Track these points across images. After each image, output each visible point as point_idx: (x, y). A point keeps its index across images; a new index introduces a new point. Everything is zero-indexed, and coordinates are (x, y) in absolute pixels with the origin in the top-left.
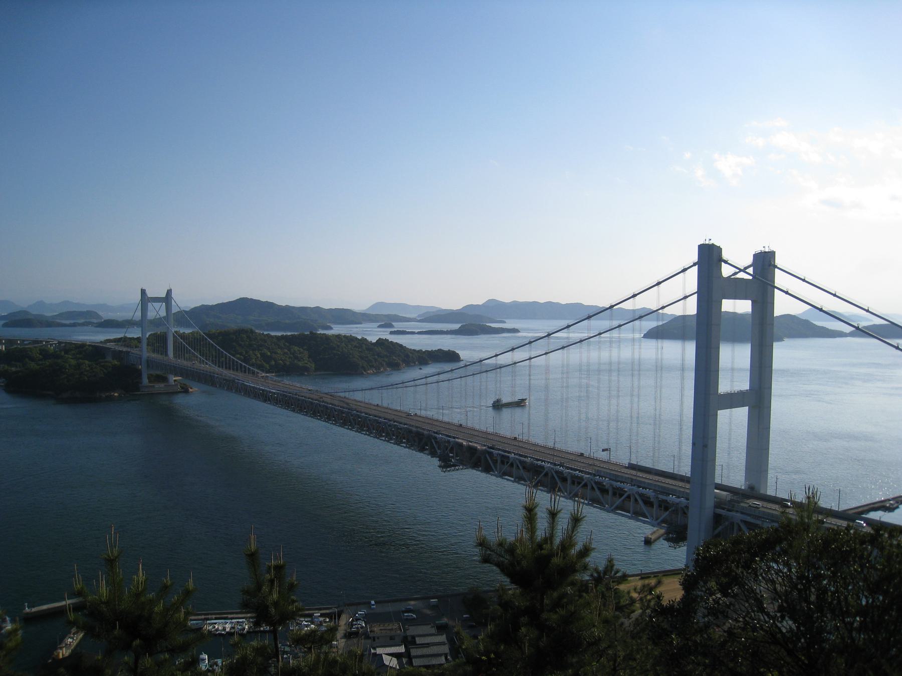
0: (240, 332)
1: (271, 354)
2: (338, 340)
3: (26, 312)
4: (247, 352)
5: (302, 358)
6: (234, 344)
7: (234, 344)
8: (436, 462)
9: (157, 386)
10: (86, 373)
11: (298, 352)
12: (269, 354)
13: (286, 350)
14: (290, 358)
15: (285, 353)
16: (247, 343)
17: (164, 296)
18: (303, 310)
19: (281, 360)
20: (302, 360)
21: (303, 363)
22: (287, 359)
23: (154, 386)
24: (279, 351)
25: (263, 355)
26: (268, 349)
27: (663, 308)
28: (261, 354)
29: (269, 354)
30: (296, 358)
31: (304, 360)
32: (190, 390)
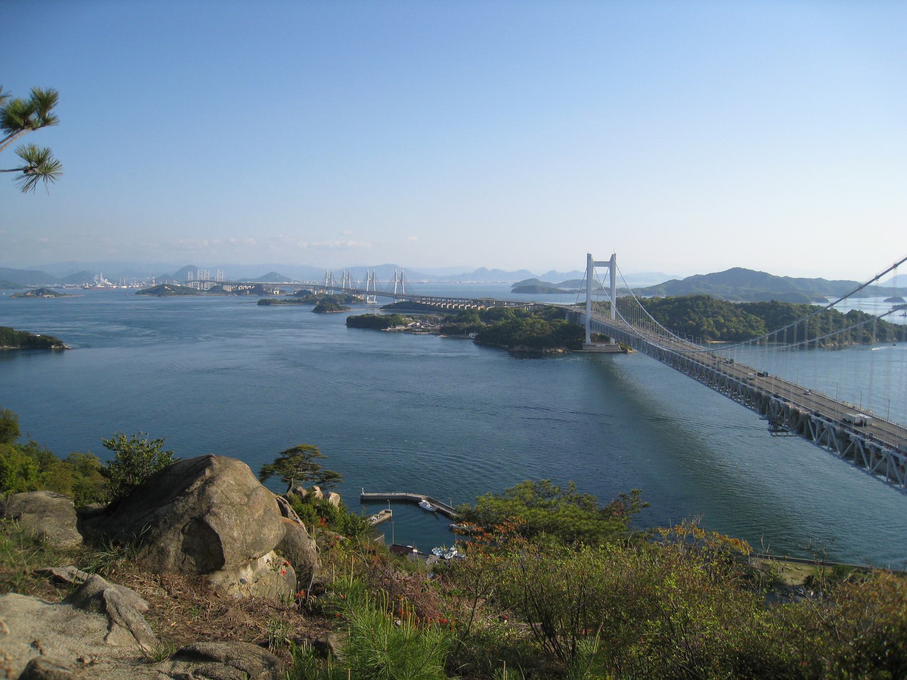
0: (698, 298)
1: (725, 321)
2: (802, 310)
3: (535, 280)
4: (700, 318)
5: (758, 327)
6: (689, 310)
7: (689, 310)
8: (765, 424)
9: (598, 345)
10: (536, 330)
11: (754, 321)
12: (722, 321)
13: (742, 318)
14: (744, 326)
15: (740, 321)
16: (702, 309)
17: (608, 260)
18: (801, 281)
19: (734, 328)
20: (757, 329)
21: (756, 331)
22: (741, 327)
23: (595, 345)
24: (734, 319)
25: (716, 322)
26: (723, 316)
27: (877, 278)
28: (714, 321)
29: (722, 321)
30: (752, 327)
31: (759, 329)
32: (629, 351)
